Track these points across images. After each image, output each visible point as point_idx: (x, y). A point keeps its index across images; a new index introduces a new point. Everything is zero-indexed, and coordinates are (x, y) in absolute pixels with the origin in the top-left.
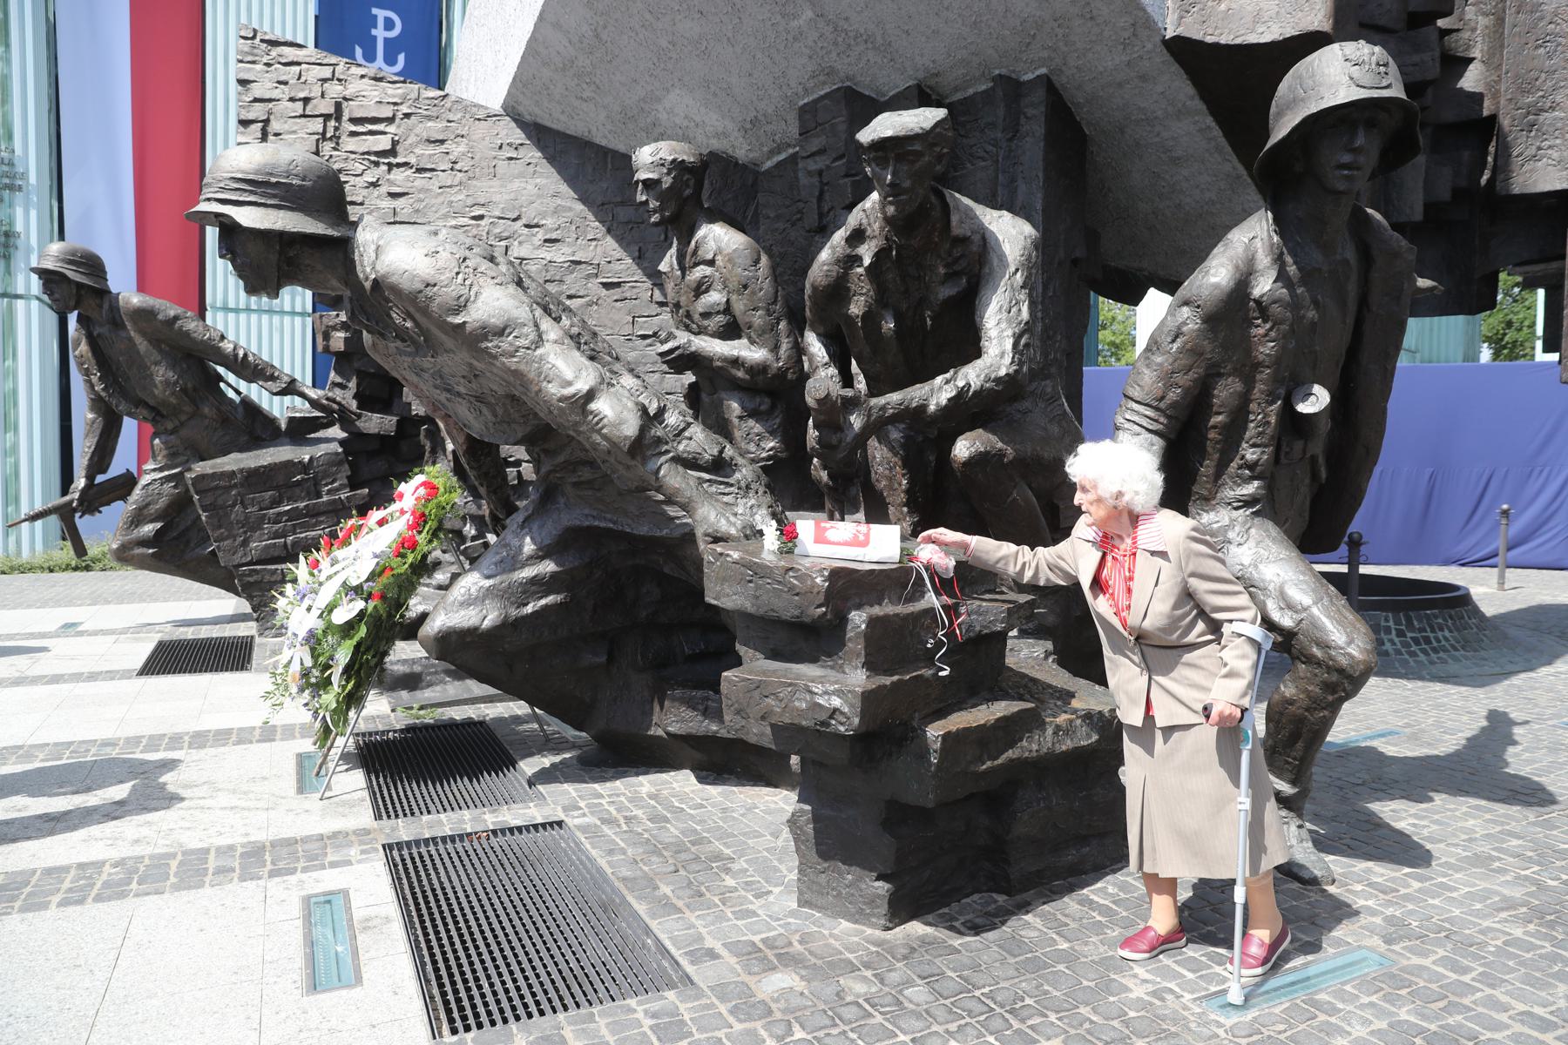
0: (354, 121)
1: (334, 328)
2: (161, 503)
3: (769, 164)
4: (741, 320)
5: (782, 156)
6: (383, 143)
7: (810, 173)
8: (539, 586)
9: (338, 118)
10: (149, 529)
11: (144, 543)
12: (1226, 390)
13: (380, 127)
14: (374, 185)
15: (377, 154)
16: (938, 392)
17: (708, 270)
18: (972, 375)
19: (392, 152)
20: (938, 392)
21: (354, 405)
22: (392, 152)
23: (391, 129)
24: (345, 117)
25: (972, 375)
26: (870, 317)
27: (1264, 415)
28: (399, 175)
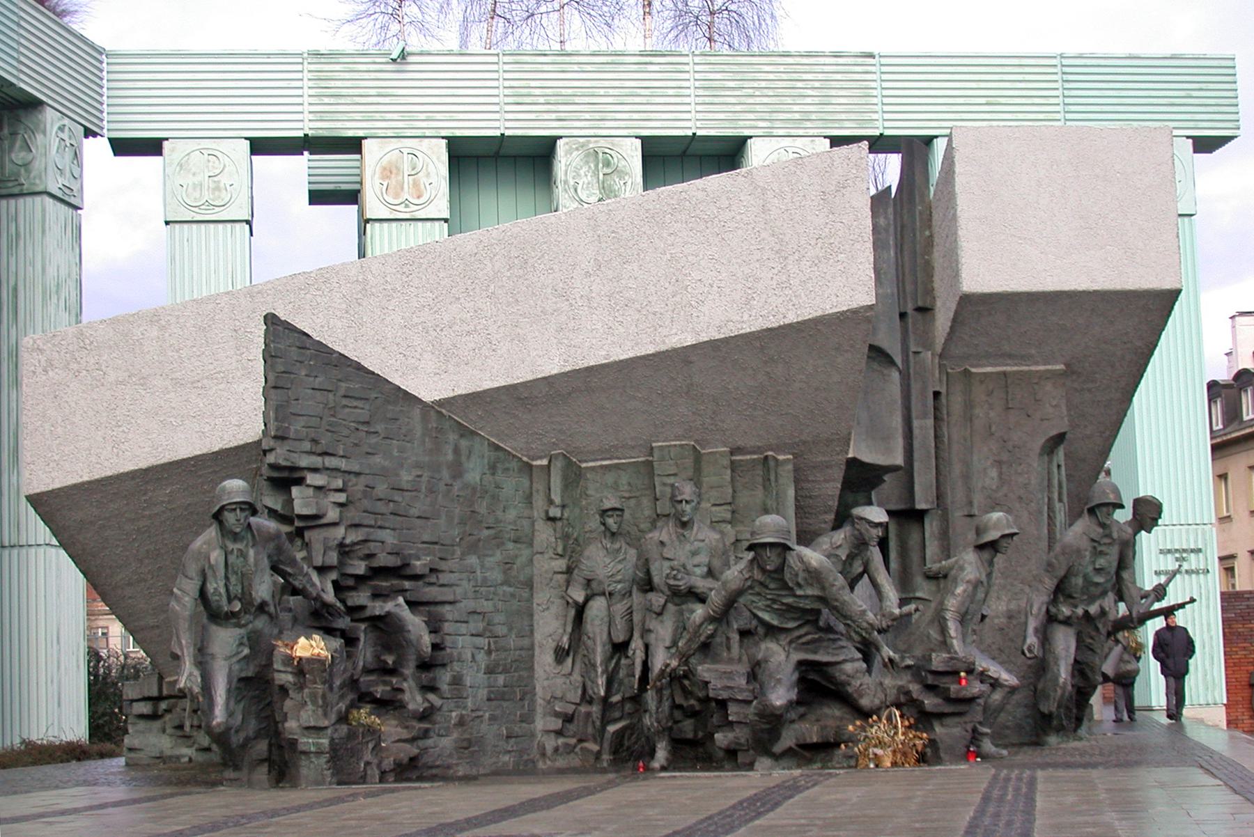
0: (345, 396)
1: (330, 548)
6: (364, 414)
7: (665, 484)
14: (356, 445)
15: (359, 422)
17: (701, 544)
19: (367, 423)
28: (373, 440)
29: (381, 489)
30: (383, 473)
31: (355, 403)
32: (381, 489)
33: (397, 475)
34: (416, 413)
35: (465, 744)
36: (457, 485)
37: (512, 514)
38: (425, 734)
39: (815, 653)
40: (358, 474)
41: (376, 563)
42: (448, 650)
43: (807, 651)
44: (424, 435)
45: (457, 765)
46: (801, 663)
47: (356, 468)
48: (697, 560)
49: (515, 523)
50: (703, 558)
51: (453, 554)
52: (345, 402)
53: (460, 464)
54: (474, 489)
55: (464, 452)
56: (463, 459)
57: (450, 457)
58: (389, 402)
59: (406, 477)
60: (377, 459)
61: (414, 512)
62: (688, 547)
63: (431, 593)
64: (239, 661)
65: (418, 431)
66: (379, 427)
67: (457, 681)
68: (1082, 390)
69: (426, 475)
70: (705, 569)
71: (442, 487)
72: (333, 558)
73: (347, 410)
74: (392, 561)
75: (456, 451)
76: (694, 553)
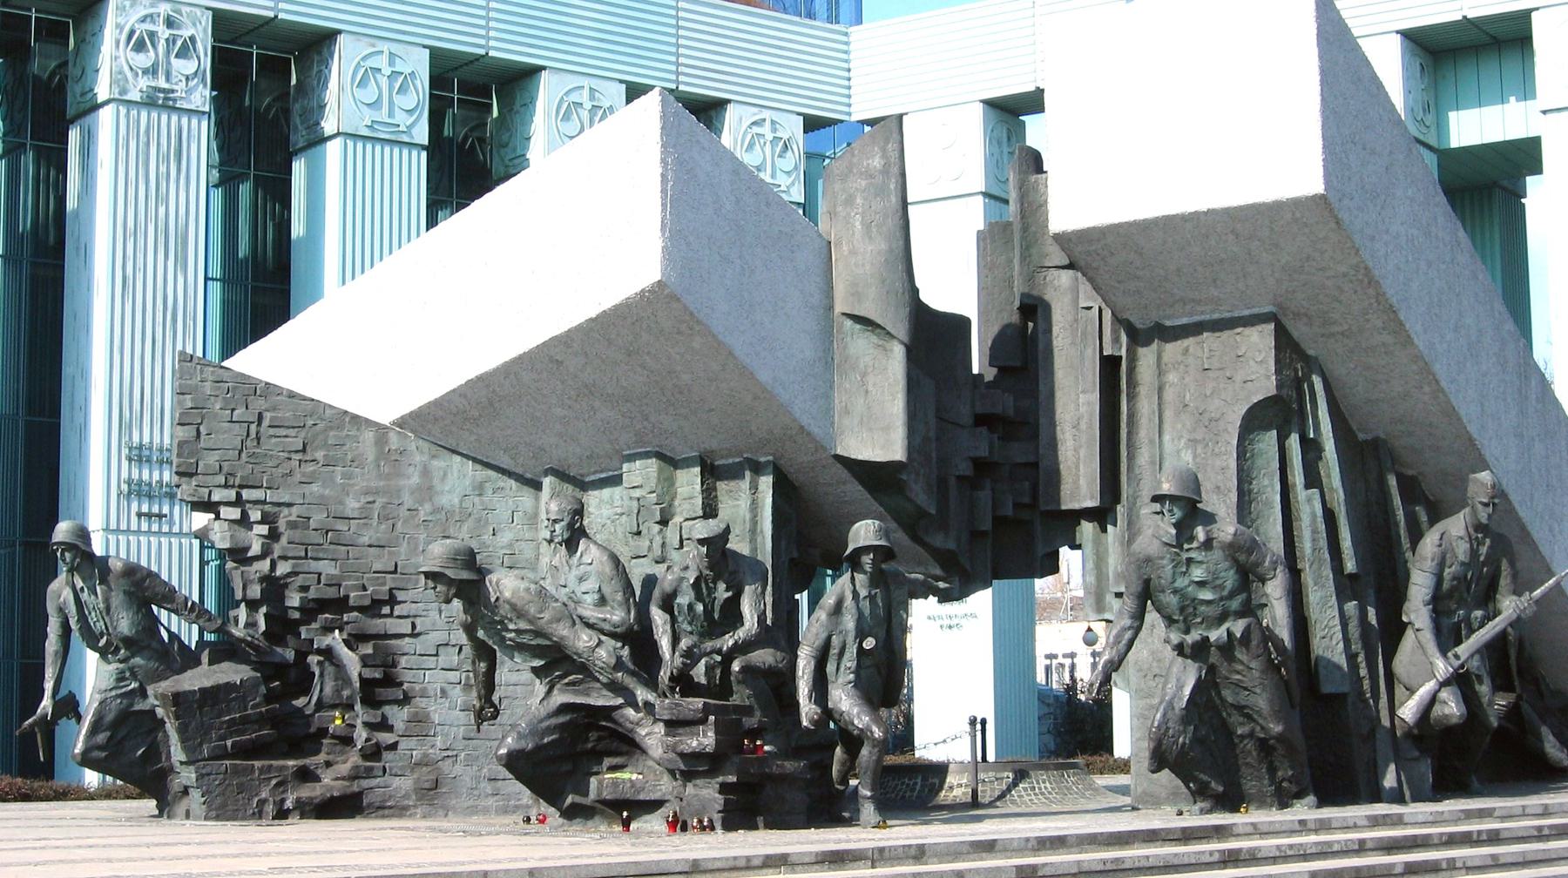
2: (110, 717)
3: (592, 478)
4: (608, 596)
5: (603, 475)
8: (549, 730)
9: (259, 424)
10: (101, 738)
11: (100, 748)
12: (835, 640)
13: (292, 432)
16: (728, 641)
18: (741, 634)
20: (728, 641)
21: (263, 643)
22: (304, 450)
23: (303, 434)
24: (266, 423)
25: (741, 634)
26: (690, 607)
27: (852, 651)
28: (310, 468)
29: (318, 518)
30: (322, 502)
31: (283, 432)
32: (318, 518)
33: (341, 503)
34: (369, 436)
35: (427, 785)
36: (428, 507)
37: (505, 537)
38: (369, 773)
39: (588, 695)
40: (290, 505)
41: (312, 594)
42: (405, 686)
43: (576, 693)
44: (377, 459)
45: (415, 806)
46: (565, 708)
47: (286, 499)
48: (585, 586)
49: (510, 545)
50: (591, 584)
51: (417, 582)
52: (272, 431)
53: (430, 488)
54: (449, 514)
55: (437, 476)
56: (436, 482)
57: (415, 479)
58: (331, 428)
59: (352, 505)
60: (315, 488)
61: (365, 540)
62: (575, 572)
63: (377, 625)
64: (117, 696)
65: (370, 454)
66: (319, 455)
67: (420, 722)
68: (1333, 335)
69: (380, 501)
70: (596, 596)
71: (403, 512)
72: (255, 591)
73: (274, 440)
74: (331, 593)
75: (426, 472)
76: (581, 579)
